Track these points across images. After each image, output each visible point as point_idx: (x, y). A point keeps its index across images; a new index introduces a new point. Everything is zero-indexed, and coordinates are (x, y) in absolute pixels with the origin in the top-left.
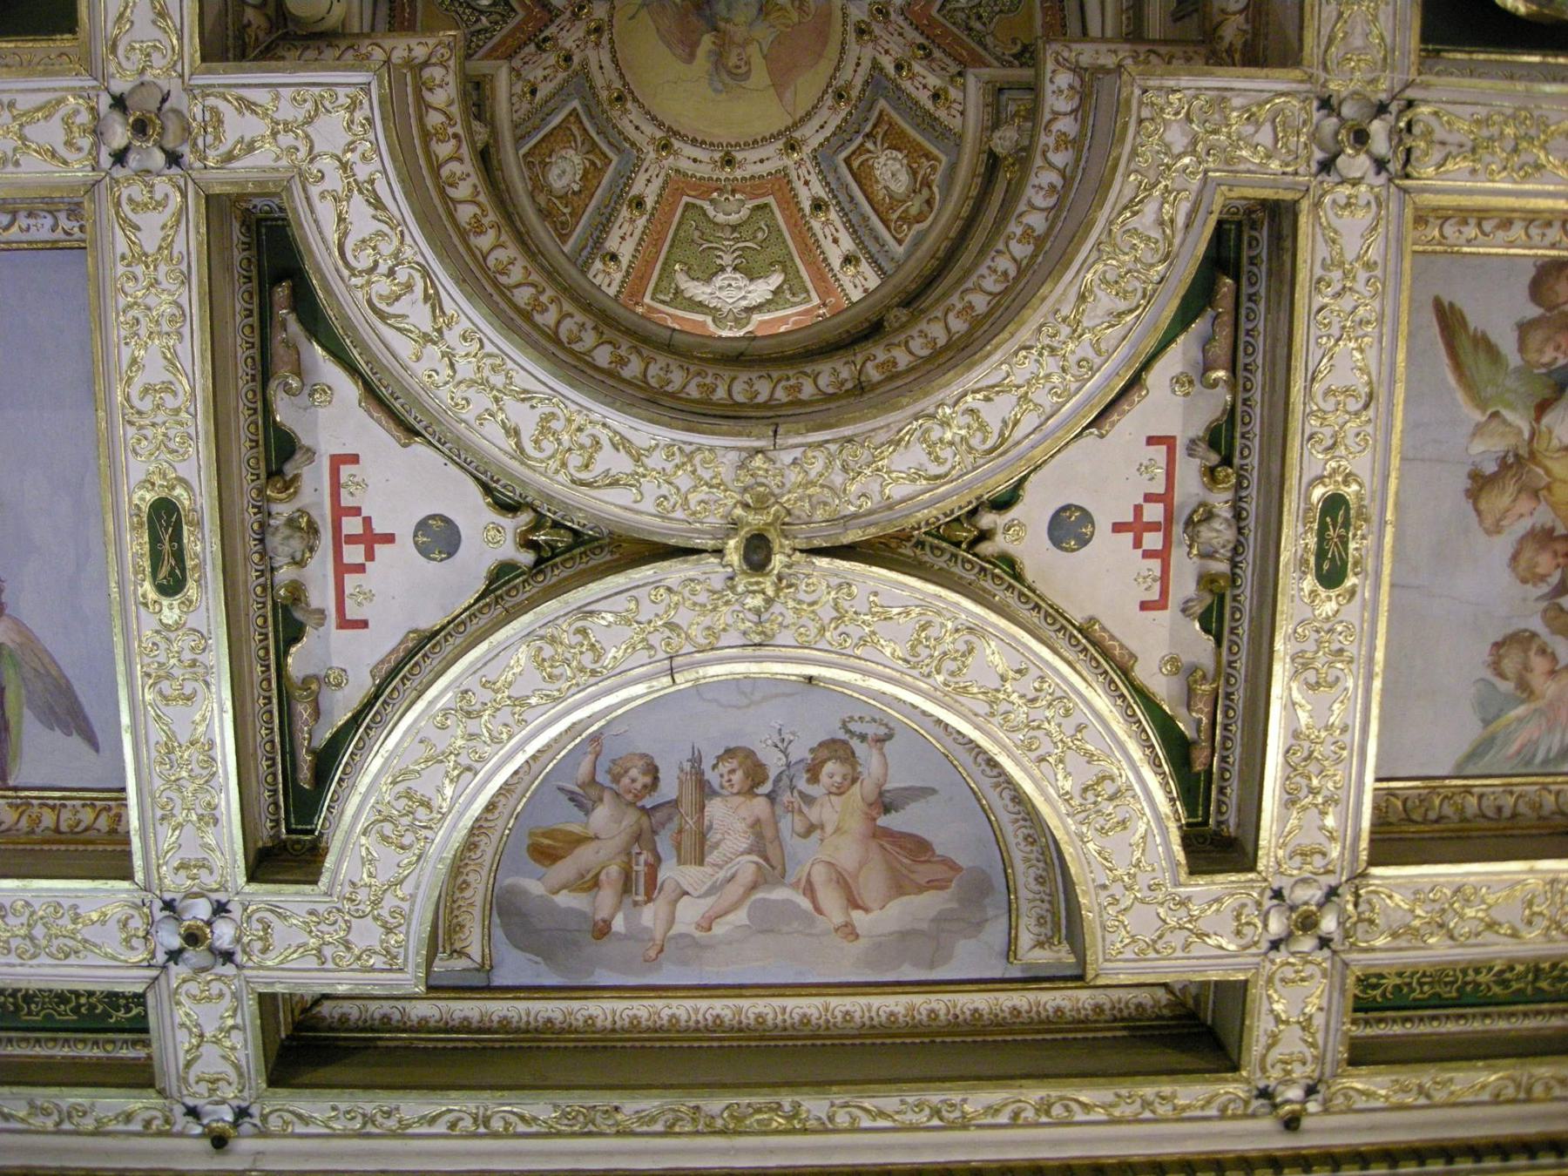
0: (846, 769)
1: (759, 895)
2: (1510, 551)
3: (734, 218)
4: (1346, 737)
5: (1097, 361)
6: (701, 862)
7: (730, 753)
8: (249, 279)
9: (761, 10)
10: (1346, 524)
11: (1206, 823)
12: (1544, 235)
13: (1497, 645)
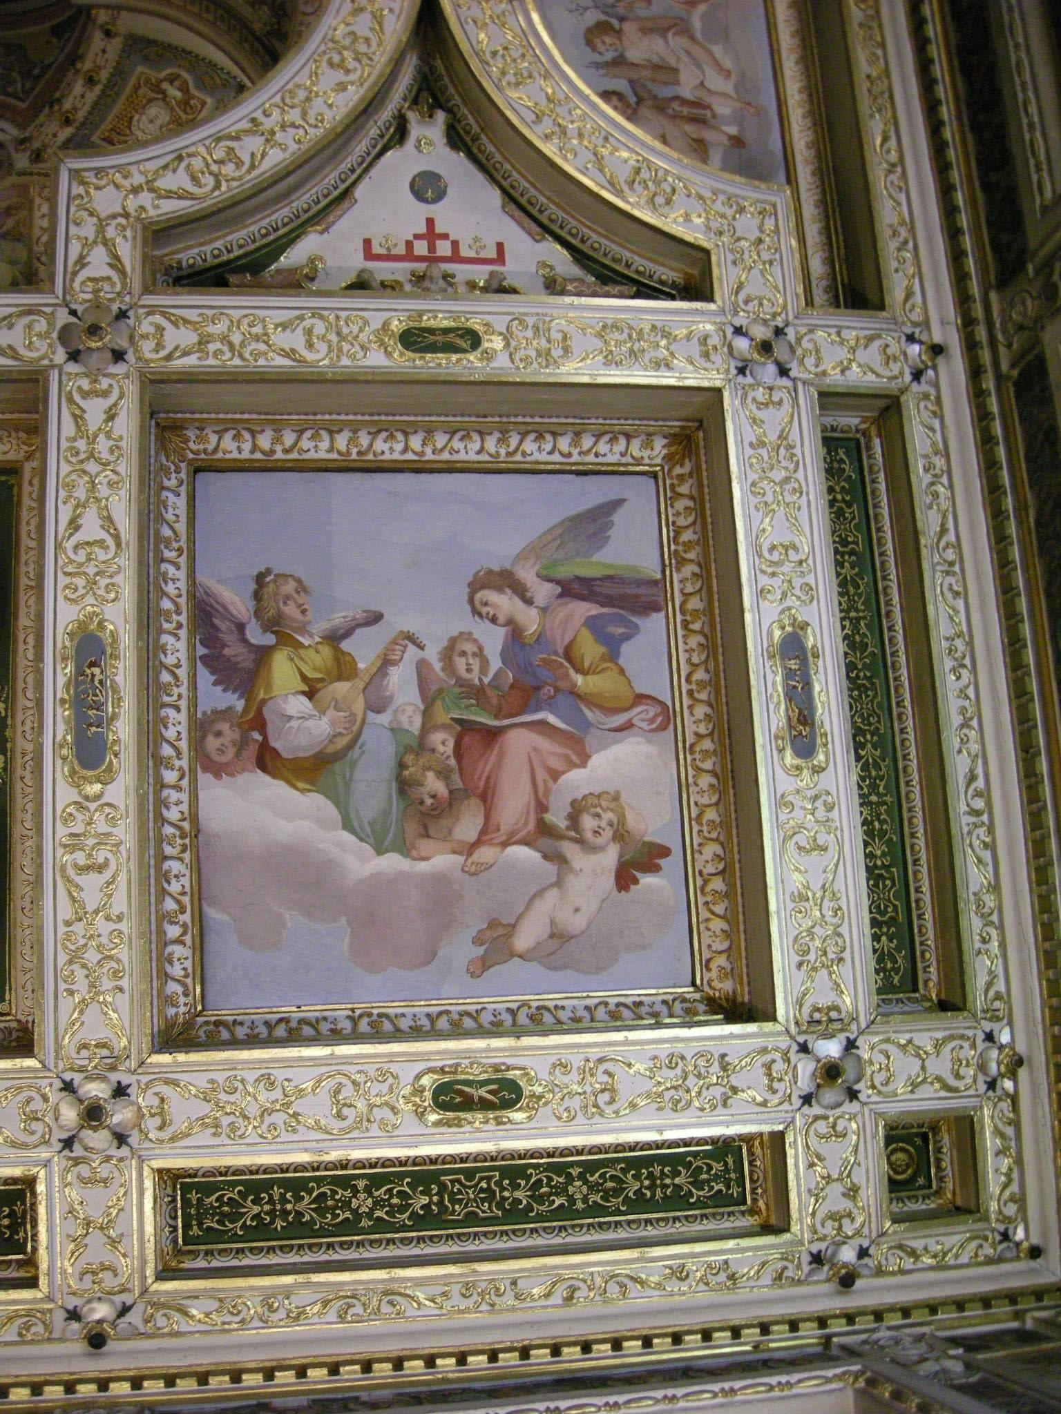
1: (698, 35)
6: (676, 71)
7: (589, 43)
9: (18, 240)
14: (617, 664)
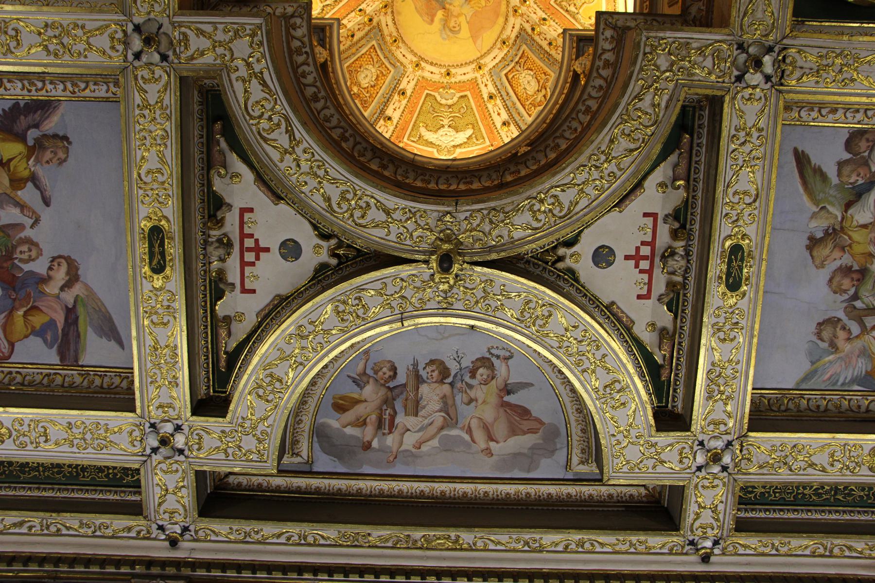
0: (489, 372)
1: (444, 432)
2: (828, 277)
3: (450, 102)
4: (739, 367)
5: (619, 173)
6: (416, 415)
7: (432, 362)
8: (202, 120)
10: (742, 260)
11: (667, 406)
12: (854, 117)
13: (819, 324)
14: (30, 334)
